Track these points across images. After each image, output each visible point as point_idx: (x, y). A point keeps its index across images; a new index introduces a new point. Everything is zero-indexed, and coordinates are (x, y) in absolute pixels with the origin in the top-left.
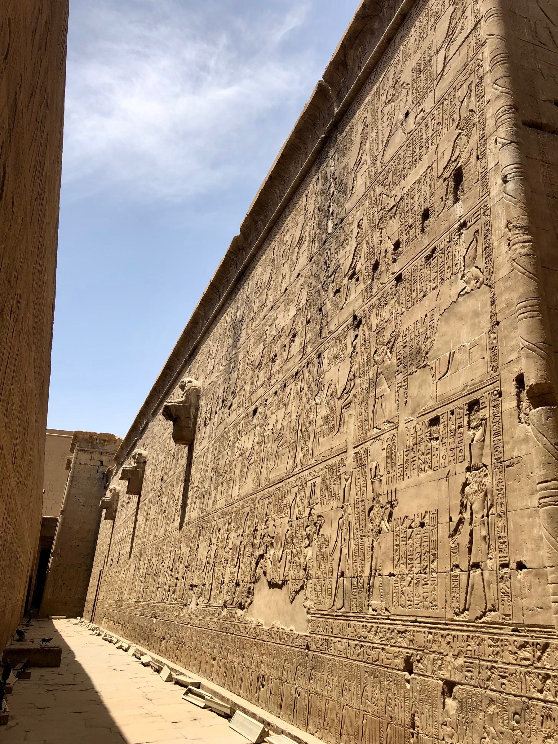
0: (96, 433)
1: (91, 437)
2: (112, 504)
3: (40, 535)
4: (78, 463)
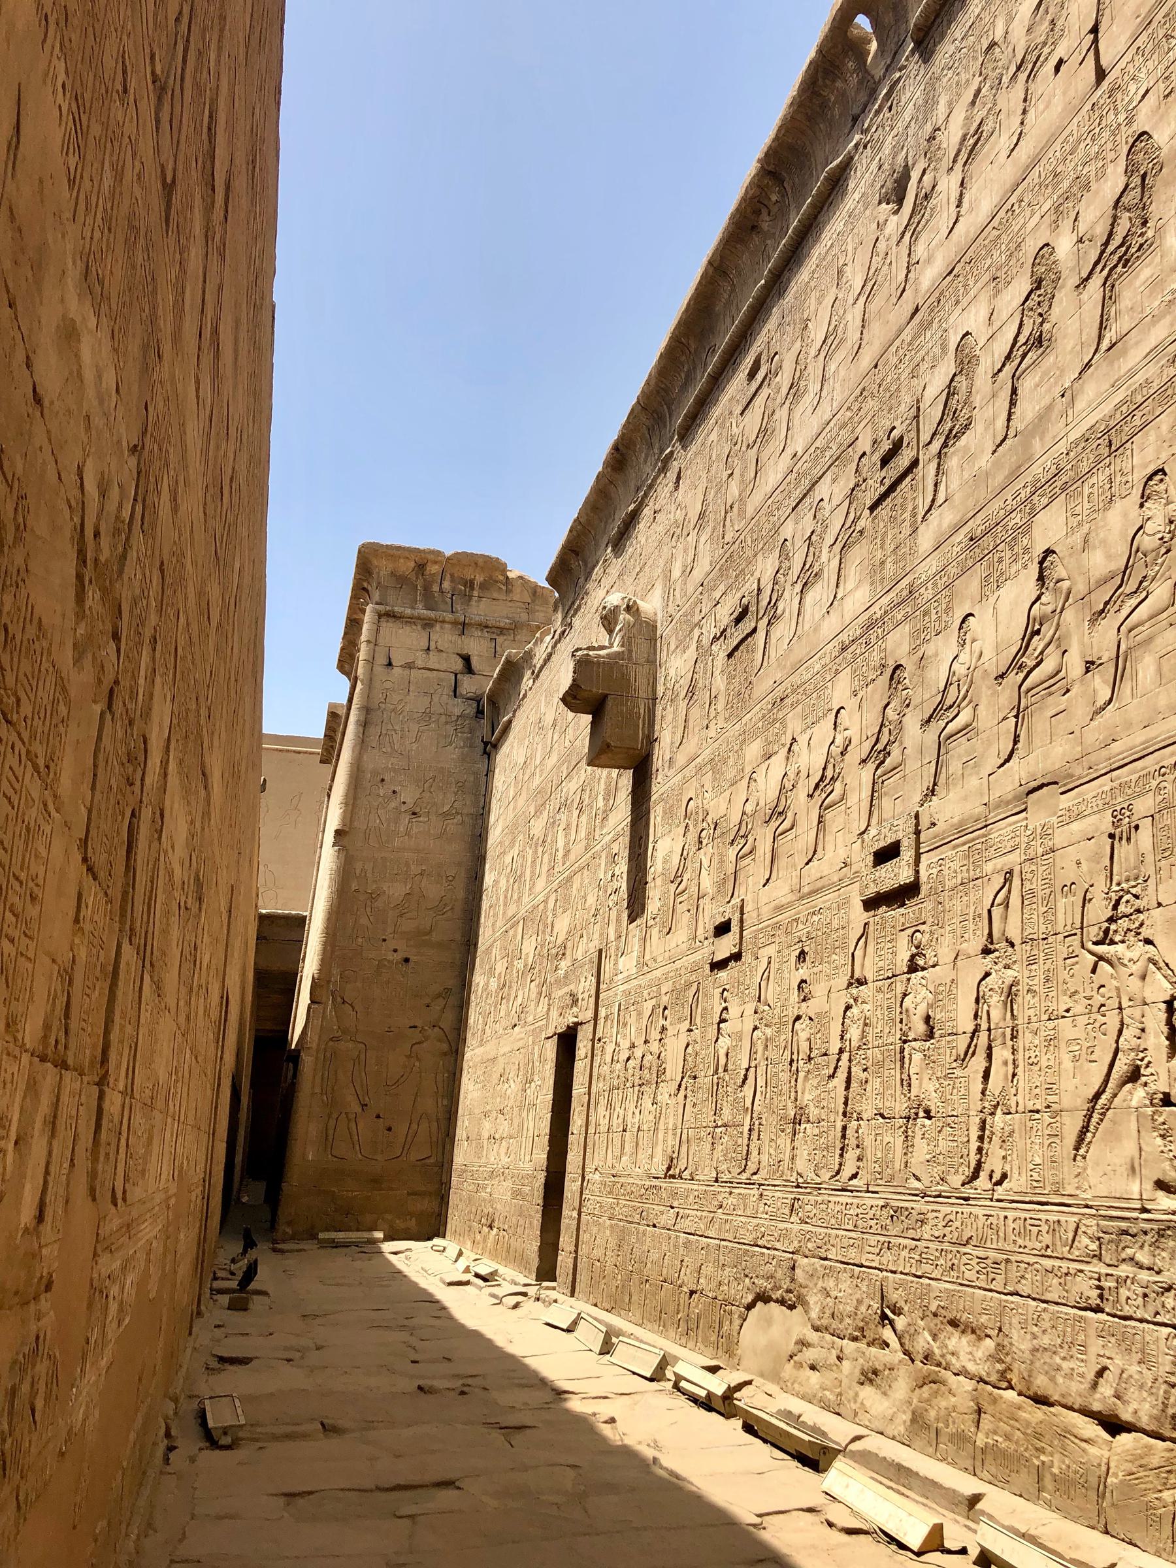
0: (438, 553)
1: (421, 567)
2: (625, 681)
3: (255, 969)
4: (381, 660)
